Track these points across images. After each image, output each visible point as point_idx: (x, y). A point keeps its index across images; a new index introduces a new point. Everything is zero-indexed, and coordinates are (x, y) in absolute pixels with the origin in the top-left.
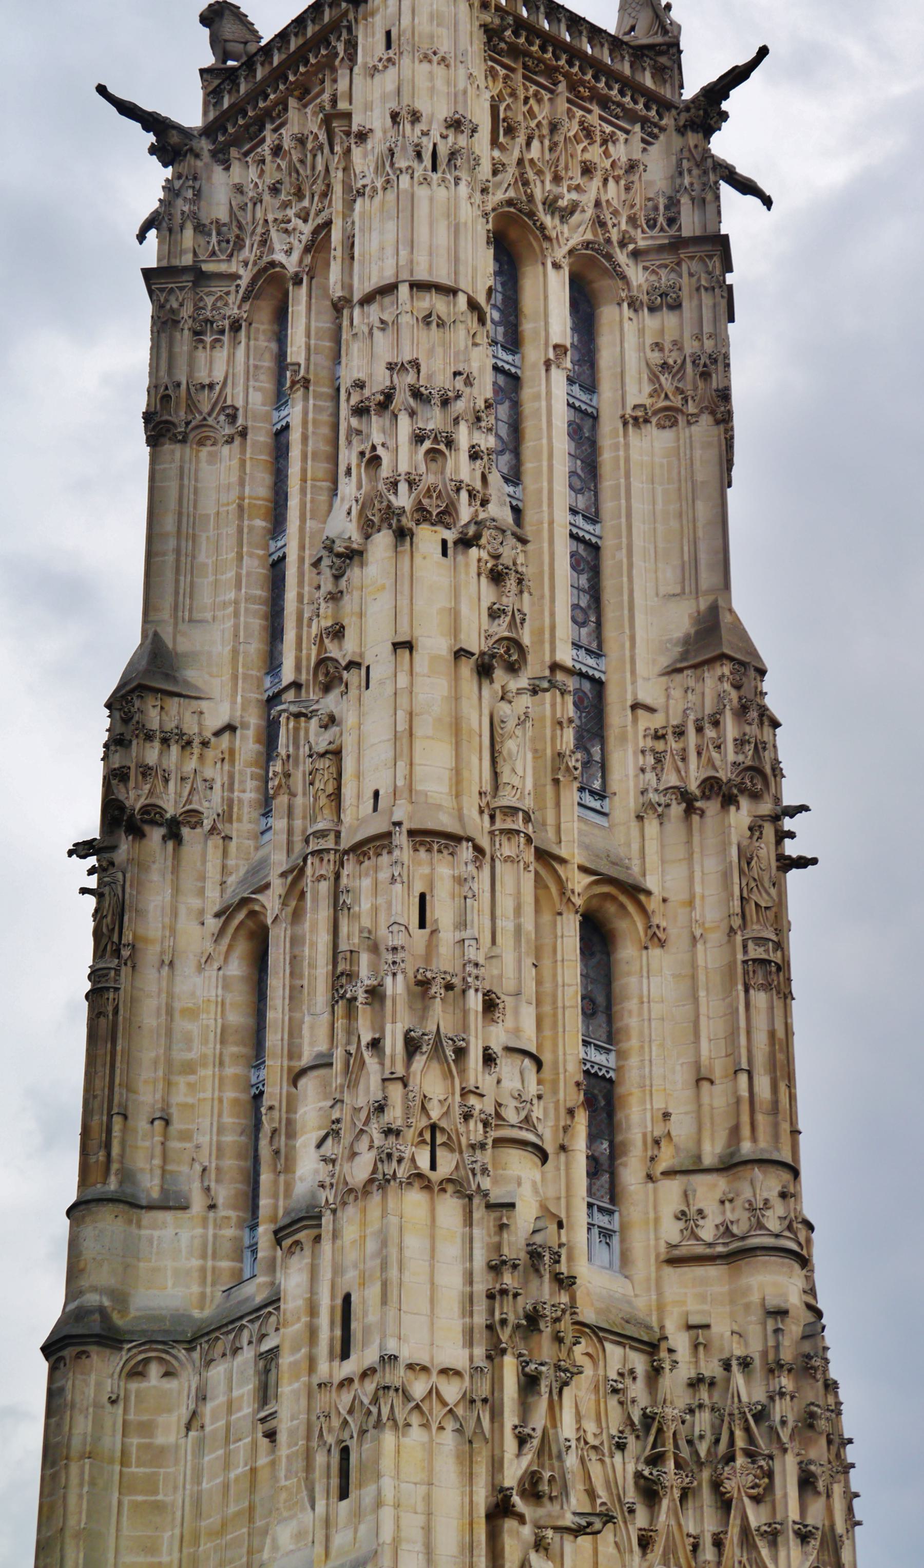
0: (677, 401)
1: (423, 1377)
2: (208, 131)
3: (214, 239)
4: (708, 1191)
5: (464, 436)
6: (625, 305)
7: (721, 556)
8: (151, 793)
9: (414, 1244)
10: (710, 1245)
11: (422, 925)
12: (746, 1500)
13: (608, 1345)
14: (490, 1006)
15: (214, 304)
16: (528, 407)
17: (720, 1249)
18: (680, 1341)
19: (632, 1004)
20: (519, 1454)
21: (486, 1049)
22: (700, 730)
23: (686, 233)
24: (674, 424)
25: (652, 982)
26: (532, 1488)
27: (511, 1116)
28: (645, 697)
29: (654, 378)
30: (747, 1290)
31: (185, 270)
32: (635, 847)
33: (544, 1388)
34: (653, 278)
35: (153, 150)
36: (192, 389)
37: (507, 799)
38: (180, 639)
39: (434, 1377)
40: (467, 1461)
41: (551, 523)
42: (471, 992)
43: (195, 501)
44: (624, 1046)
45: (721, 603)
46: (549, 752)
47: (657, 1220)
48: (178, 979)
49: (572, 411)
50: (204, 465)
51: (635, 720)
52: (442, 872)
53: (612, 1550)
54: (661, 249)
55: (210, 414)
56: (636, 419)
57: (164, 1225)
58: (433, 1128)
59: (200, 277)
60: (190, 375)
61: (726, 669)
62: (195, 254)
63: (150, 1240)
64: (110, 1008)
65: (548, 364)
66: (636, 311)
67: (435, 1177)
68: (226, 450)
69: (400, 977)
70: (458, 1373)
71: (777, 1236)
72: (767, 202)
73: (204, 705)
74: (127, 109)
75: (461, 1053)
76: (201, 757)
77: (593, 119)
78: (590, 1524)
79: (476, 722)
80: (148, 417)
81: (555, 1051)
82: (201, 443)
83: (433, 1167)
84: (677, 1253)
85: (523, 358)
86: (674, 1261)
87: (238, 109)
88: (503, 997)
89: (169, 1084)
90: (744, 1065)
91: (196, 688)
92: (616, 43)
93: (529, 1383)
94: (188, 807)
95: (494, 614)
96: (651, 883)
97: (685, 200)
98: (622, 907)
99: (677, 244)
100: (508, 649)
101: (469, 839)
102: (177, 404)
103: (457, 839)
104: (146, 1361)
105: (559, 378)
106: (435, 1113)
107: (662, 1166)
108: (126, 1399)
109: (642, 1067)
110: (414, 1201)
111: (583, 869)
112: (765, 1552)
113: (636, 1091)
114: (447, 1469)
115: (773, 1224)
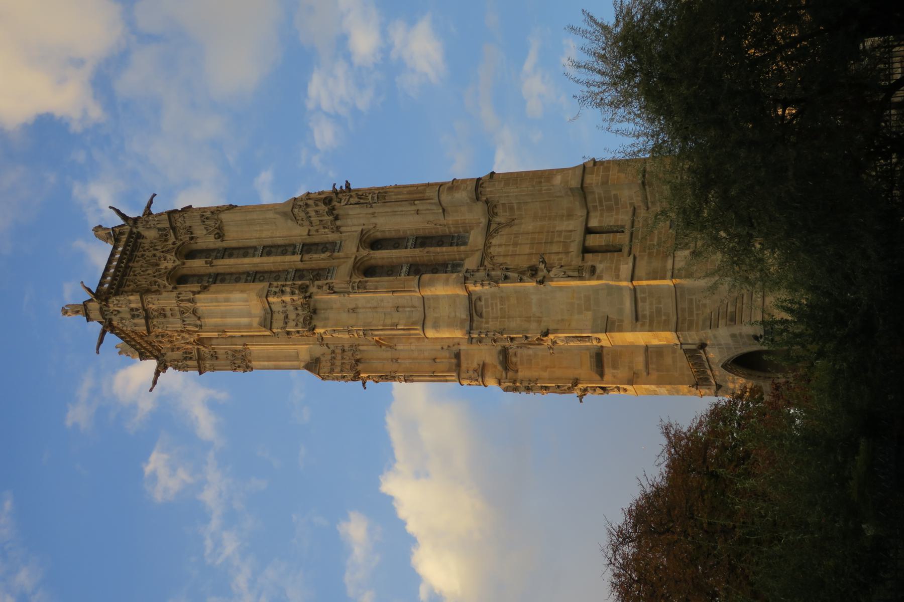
2: (157, 358)
23: (168, 225)
31: (198, 362)
35: (164, 372)
54: (175, 233)
74: (155, 382)
77: (139, 254)
87: (150, 352)
92: (115, 248)
96: (360, 229)
97: (159, 226)
99: (173, 228)
105: (215, 262)
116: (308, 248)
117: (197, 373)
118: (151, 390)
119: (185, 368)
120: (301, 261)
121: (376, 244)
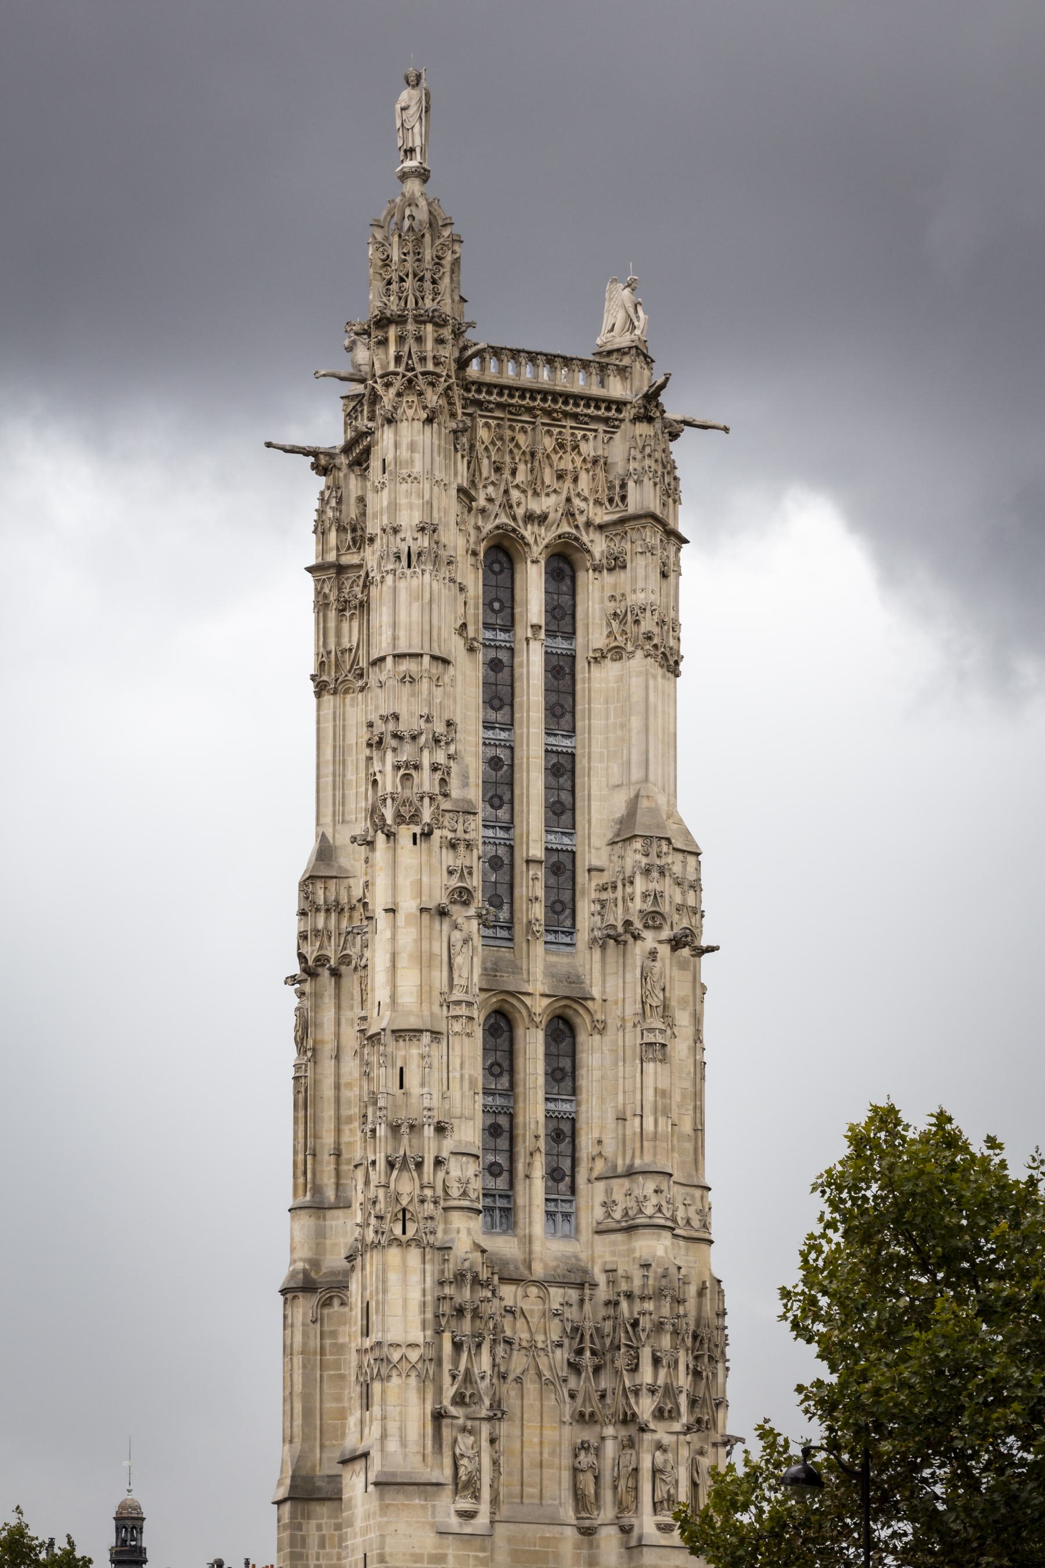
0: (620, 641)
1: (399, 1349)
2: (347, 450)
3: (349, 537)
4: (619, 1187)
5: (426, 761)
6: (591, 571)
7: (644, 757)
8: (321, 947)
9: (393, 1277)
10: (618, 1222)
11: (401, 1087)
13: (550, 1289)
14: (441, 1129)
15: (351, 587)
16: (517, 672)
17: (623, 1224)
18: (601, 1278)
20: (452, 1384)
21: (437, 1157)
22: (624, 885)
24: (621, 658)
25: (595, 1056)
26: (459, 1400)
27: (455, 1192)
28: (596, 862)
29: (609, 624)
30: (633, 1250)
32: (588, 967)
33: (465, 1348)
34: (612, 545)
36: (339, 654)
37: (457, 995)
38: (337, 836)
39: (404, 1350)
40: (422, 1392)
41: (528, 758)
42: (426, 1127)
43: (344, 735)
44: (579, 1097)
45: (643, 793)
46: (525, 920)
47: (592, 1207)
48: (342, 1064)
49: (671, 524)
50: (348, 708)
51: (590, 880)
52: (410, 1054)
53: (553, 1403)
55: (350, 672)
56: (595, 658)
57: (338, 1218)
58: (404, 1210)
59: (341, 569)
60: (338, 644)
61: (638, 844)
62: (338, 549)
63: (331, 1228)
64: (303, 1089)
65: (527, 640)
66: (600, 572)
67: (404, 1238)
68: (360, 695)
69: (383, 1125)
70: (417, 1345)
71: (650, 1217)
73: (351, 881)
75: (419, 1165)
76: (351, 917)
78: (495, 1415)
79: (440, 948)
80: (313, 678)
81: (525, 1117)
82: (346, 692)
83: (404, 1233)
84: (601, 1227)
85: (514, 635)
86: (598, 1232)
88: (453, 1121)
89: (338, 1131)
90: (638, 1112)
91: (347, 871)
93: (457, 1346)
94: (344, 953)
95: (450, 873)
96: (596, 992)
100: (460, 893)
102: (330, 667)
103: (421, 1031)
104: (331, 1298)
106: (404, 1202)
107: (595, 1174)
108: (322, 1319)
109: (587, 1112)
110: (394, 1254)
111: (543, 995)
112: (632, 1401)
113: (584, 1126)
114: (413, 1396)
115: (649, 1210)
116: (561, 867)
117: (312, 562)
119: (321, 530)
120: (528, 862)
121: (562, 1030)
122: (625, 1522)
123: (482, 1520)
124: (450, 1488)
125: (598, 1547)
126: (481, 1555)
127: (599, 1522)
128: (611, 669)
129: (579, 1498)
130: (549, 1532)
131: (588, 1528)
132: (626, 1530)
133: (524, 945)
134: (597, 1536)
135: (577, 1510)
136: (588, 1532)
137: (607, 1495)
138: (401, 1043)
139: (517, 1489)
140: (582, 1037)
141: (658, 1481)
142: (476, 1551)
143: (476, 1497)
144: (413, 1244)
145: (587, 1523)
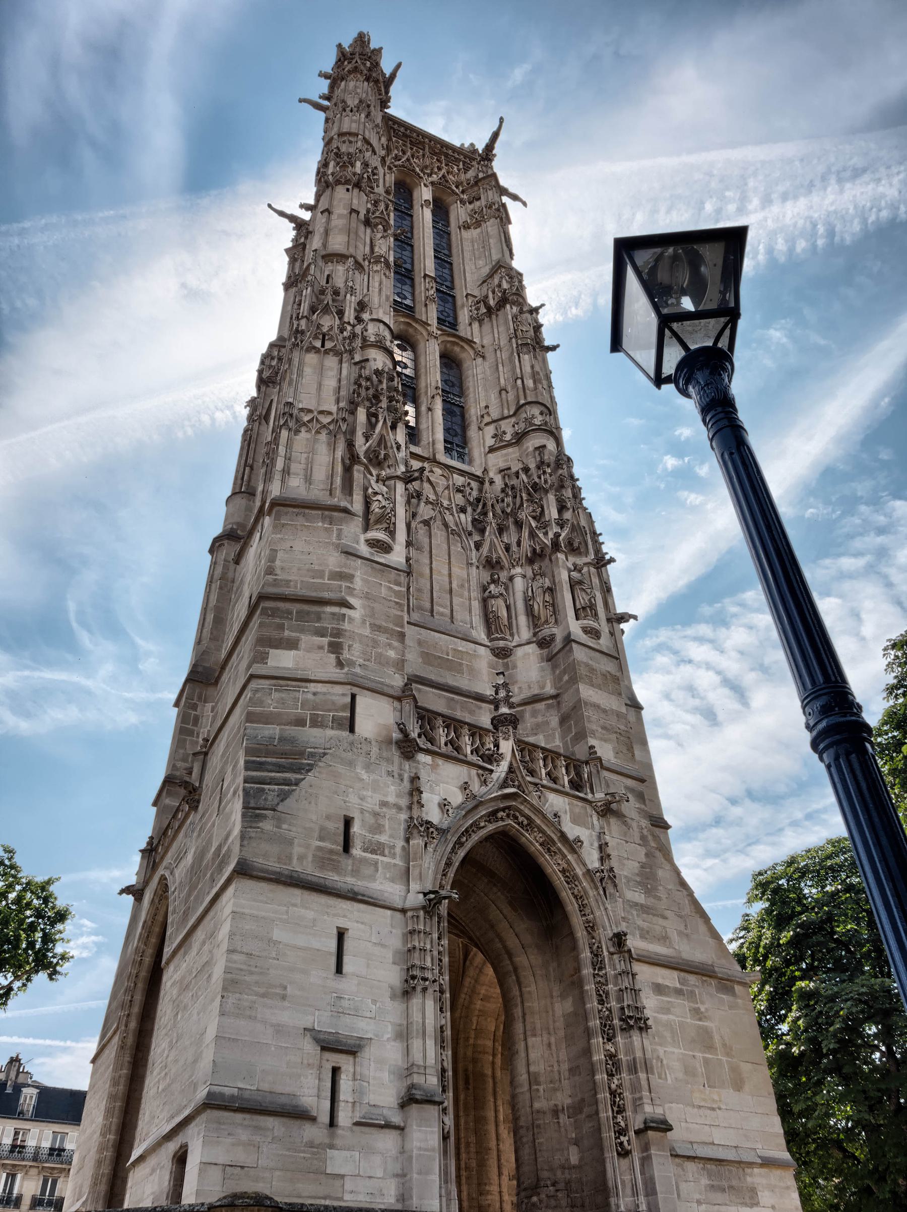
9: (308, 370)
12: (530, 518)
19: (471, 379)
72: (525, 204)
93: (372, 416)
98: (462, 347)
101: (351, 256)
118: (270, 206)
120: (426, 276)
122: (546, 632)
123: (397, 556)
124: (359, 521)
125: (515, 667)
126: (396, 588)
127: (514, 644)
128: (474, 233)
129: (490, 621)
130: (463, 646)
131: (503, 649)
132: (544, 643)
133: (424, 309)
134: (512, 658)
135: (489, 633)
136: (502, 654)
137: (522, 620)
138: (330, 264)
139: (428, 605)
140: (467, 364)
141: (578, 592)
142: (389, 582)
143: (392, 533)
144: (331, 353)
145: (501, 644)
